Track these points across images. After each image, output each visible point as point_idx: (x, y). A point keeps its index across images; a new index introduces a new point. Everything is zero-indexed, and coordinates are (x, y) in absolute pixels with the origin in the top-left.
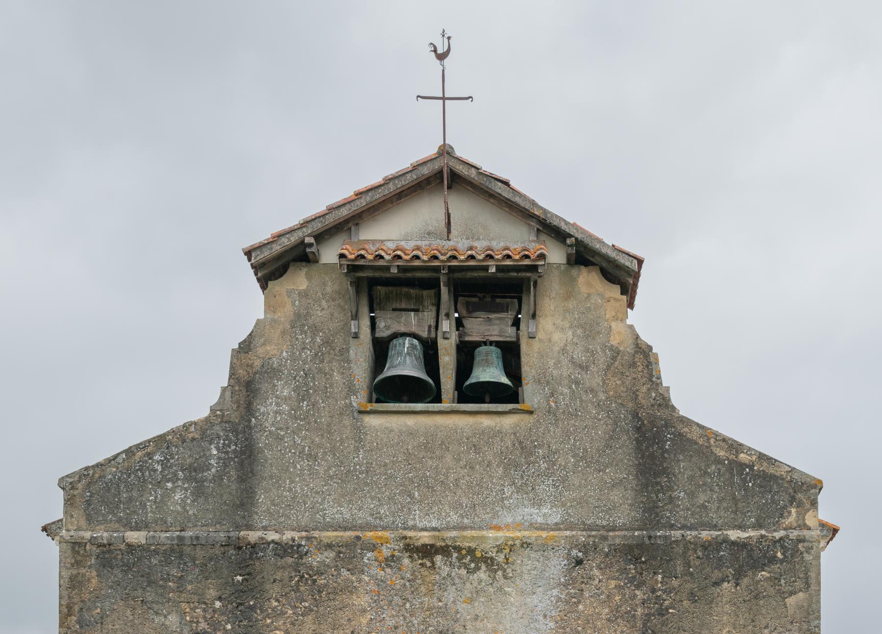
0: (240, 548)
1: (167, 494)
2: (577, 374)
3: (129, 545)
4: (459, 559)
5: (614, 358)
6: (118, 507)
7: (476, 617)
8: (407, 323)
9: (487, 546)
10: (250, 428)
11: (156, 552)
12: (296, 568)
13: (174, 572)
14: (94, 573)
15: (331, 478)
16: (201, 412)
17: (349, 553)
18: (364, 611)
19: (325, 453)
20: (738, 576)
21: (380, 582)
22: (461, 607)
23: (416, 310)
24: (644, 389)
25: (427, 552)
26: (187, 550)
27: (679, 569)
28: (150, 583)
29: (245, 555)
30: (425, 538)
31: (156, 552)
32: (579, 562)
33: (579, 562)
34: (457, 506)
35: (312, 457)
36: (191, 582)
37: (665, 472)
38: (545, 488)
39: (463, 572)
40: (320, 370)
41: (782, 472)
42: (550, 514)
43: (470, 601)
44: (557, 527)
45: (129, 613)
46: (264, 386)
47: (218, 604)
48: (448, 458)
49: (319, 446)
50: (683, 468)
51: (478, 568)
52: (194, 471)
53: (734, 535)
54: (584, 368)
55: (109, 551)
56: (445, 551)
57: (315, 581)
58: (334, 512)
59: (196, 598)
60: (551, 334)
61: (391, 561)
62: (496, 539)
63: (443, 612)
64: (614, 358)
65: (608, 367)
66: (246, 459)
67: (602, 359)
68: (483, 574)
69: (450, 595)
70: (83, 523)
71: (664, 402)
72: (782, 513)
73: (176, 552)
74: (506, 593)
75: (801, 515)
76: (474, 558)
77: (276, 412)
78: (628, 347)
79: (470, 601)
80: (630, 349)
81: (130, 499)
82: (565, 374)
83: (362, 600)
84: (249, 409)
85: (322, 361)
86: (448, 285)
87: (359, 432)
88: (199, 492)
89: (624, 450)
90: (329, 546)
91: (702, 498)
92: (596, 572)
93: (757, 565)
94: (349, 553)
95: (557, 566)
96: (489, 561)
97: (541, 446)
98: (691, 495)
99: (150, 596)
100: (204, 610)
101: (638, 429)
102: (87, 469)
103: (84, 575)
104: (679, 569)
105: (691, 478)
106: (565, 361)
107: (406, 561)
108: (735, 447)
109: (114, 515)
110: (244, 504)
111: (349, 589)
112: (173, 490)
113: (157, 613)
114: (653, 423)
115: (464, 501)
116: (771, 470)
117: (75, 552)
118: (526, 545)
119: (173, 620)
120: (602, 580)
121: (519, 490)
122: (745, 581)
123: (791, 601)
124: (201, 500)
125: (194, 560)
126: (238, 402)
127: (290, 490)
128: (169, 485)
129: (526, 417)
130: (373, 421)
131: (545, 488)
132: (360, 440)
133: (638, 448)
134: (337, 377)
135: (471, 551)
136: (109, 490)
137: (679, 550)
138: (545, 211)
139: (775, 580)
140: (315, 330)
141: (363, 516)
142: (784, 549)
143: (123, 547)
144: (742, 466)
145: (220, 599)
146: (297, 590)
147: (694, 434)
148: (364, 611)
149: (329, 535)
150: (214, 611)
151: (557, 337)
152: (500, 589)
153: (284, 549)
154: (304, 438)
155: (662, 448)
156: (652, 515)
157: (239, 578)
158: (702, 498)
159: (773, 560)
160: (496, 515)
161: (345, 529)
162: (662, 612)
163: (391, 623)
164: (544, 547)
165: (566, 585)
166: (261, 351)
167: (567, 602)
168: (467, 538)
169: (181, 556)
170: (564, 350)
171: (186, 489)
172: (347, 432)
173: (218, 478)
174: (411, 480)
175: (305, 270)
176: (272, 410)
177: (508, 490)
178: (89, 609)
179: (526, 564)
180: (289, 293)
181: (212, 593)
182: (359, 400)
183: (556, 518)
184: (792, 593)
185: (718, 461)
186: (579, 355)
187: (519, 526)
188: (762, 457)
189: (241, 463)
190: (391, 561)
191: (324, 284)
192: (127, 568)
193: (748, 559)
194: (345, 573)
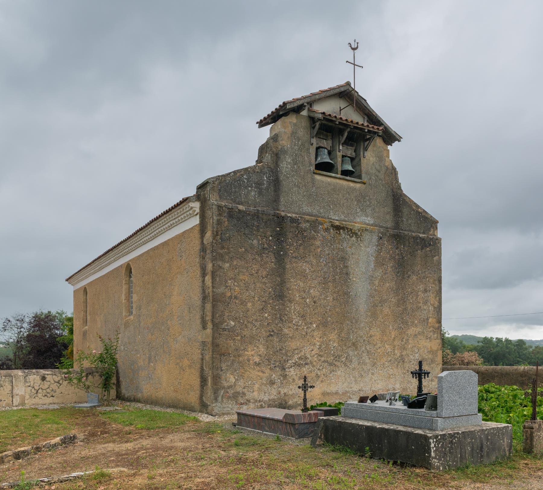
0: (278, 217)
1: (249, 192)
2: (377, 173)
3: (239, 210)
4: (348, 232)
5: (387, 170)
6: (231, 194)
7: (352, 254)
8: (323, 144)
9: (356, 228)
10: (278, 172)
11: (249, 214)
12: (297, 227)
13: (256, 223)
14: (226, 220)
15: (305, 196)
17: (314, 225)
18: (319, 247)
19: (302, 186)
20: (422, 249)
21: (323, 237)
22: (348, 249)
23: (326, 140)
24: (394, 182)
25: (338, 228)
26: (260, 215)
27: (407, 244)
28: (247, 226)
29: (281, 220)
30: (337, 223)
31: (249, 214)
32: (381, 238)
33: (381, 238)
34: (343, 213)
36: (262, 228)
37: (400, 211)
38: (369, 211)
39: (348, 237)
40: (301, 155)
41: (429, 217)
42: (369, 220)
43: (351, 247)
44: (372, 225)
45: (239, 238)
46: (282, 157)
47: (271, 238)
48: (341, 195)
49: (301, 183)
50: (405, 210)
51: (353, 236)
52: (259, 184)
53: (421, 235)
54: (379, 172)
55: (232, 211)
56: (343, 228)
57: (303, 234)
58: (306, 209)
59: (263, 235)
61: (327, 230)
62: (358, 227)
63: (343, 250)
64: (387, 170)
65: (385, 173)
67: (384, 169)
68: (354, 238)
69: (345, 245)
70: (218, 198)
71: (399, 188)
72: (429, 230)
73: (256, 215)
74: (361, 246)
75: (434, 231)
76: (352, 233)
77: (286, 167)
78: (390, 167)
79: (351, 247)
80: (391, 168)
81: (235, 192)
82: (374, 172)
83: (318, 243)
84: (277, 165)
85: (301, 151)
86: (349, 133)
87: (313, 179)
88: (260, 193)
90: (308, 221)
91: (410, 221)
92: (385, 242)
93: (426, 247)
94: (314, 225)
95: (375, 238)
96: (356, 234)
97: (367, 196)
98: (407, 220)
99: (247, 232)
100: (266, 240)
101: (393, 195)
102: (219, 176)
103: (222, 220)
104: (407, 244)
105: (407, 215)
106: (374, 168)
107: (332, 230)
108: (418, 206)
109: (230, 197)
110: (276, 200)
111: (314, 238)
112: (251, 191)
113: (249, 239)
114: (397, 194)
115: (345, 211)
116: (426, 216)
117: (219, 210)
118: (366, 230)
119: (255, 242)
120: (388, 245)
121: (361, 210)
122: (424, 251)
123: (435, 258)
124: (261, 196)
125: (263, 219)
126: (273, 161)
127: (291, 198)
128: (250, 188)
129: (363, 185)
130: (318, 177)
131: (369, 211)
132: (314, 184)
134: (306, 159)
135: (351, 230)
136: (228, 187)
137: (407, 238)
138: (377, 114)
139: (431, 251)
140: (299, 139)
141: (315, 212)
143: (237, 210)
144: (420, 213)
145: (271, 236)
146: (297, 236)
147: (407, 200)
148: (319, 247)
149: (307, 217)
150: (270, 240)
151: (371, 159)
152: (359, 244)
153: (293, 220)
154: (296, 179)
155: (399, 203)
156: (397, 225)
157: (278, 229)
158: (410, 221)
159: (430, 245)
160: (355, 218)
161: (312, 216)
162: (403, 258)
163: (327, 252)
164: (371, 232)
165: (378, 246)
166: (281, 142)
167: (378, 251)
168: (349, 225)
169: (258, 217)
170: (373, 164)
171: (256, 191)
172: (309, 180)
173: (267, 189)
174: (330, 201)
175: (295, 115)
176: (285, 165)
177: (358, 210)
178: (224, 234)
179: (366, 236)
180: (290, 123)
181: (269, 233)
182: (313, 168)
183: (372, 222)
184: (435, 256)
185: (414, 210)
188: (424, 211)
189: (275, 184)
190: (327, 230)
191: (302, 122)
192: (239, 219)
194: (313, 232)
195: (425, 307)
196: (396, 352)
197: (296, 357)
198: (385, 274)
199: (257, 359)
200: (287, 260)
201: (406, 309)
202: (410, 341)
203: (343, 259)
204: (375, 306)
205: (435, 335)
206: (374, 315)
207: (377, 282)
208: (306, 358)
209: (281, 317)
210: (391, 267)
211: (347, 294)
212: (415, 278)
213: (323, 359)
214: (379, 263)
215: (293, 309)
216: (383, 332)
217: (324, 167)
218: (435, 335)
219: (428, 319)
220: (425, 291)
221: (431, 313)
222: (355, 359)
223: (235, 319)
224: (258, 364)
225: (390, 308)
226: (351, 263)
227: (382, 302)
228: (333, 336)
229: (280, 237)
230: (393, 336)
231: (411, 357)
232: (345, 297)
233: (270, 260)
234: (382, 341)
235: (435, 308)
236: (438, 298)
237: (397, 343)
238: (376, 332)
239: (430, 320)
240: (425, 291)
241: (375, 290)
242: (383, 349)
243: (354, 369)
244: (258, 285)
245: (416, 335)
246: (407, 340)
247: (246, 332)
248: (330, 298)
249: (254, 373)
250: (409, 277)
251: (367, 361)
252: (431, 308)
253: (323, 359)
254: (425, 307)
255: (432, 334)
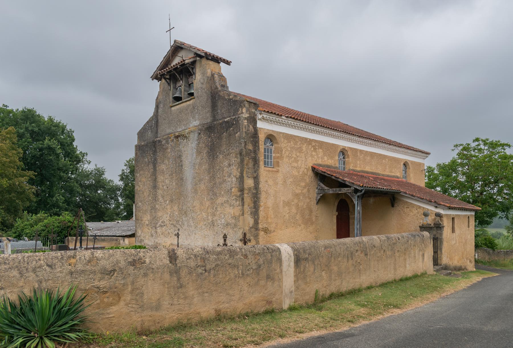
16: (152, 114)
25: (177, 137)
30: (177, 134)
34: (184, 125)
35: (165, 119)
42: (197, 123)
50: (219, 104)
53: (226, 120)
60: (199, 78)
61: (173, 140)
66: (157, 122)
68: (185, 141)
69: (181, 147)
72: (238, 111)
73: (146, 145)
76: (185, 137)
83: (169, 150)
88: (152, 132)
89: (209, 104)
93: (230, 127)
95: (197, 135)
96: (186, 137)
98: (221, 111)
101: (212, 96)
111: (167, 148)
123: (237, 135)
130: (173, 108)
133: (212, 101)
139: (233, 130)
142: (236, 121)
144: (230, 99)
149: (164, 137)
153: (160, 141)
156: (214, 119)
159: (233, 124)
179: (192, 136)
184: (237, 133)
186: (202, 81)
187: (193, 127)
190: (173, 140)
193: (228, 125)
195: (229, 179)
196: (209, 217)
197: (161, 221)
198: (202, 159)
199: (147, 222)
200: (157, 166)
201: (215, 184)
202: (218, 209)
203: (180, 157)
204: (196, 184)
205: (238, 203)
206: (196, 191)
207: (197, 167)
208: (165, 222)
209: (155, 199)
210: (206, 153)
211: (182, 179)
212: (221, 156)
213: (171, 223)
214: (199, 152)
215: (160, 192)
216: (201, 203)
217: (178, 99)
218: (238, 203)
219: (231, 189)
220: (230, 165)
221: (234, 183)
222: (186, 223)
223: (141, 202)
224: (147, 225)
225: (205, 184)
226: (183, 158)
227: (200, 180)
228: (176, 208)
229: (155, 152)
230: (207, 206)
231: (219, 221)
232: (181, 180)
233: (151, 166)
234: (200, 210)
235: (237, 178)
236: (239, 170)
237: (209, 211)
238: (197, 203)
239: (233, 190)
240: (230, 165)
241: (196, 173)
242: (201, 215)
243: (185, 230)
244: (148, 182)
245: (222, 204)
246: (216, 208)
247: (144, 209)
248: (174, 184)
249: (146, 230)
250: (217, 157)
251: (192, 224)
252: (234, 179)
253: (171, 223)
254: (229, 179)
255: (234, 201)
